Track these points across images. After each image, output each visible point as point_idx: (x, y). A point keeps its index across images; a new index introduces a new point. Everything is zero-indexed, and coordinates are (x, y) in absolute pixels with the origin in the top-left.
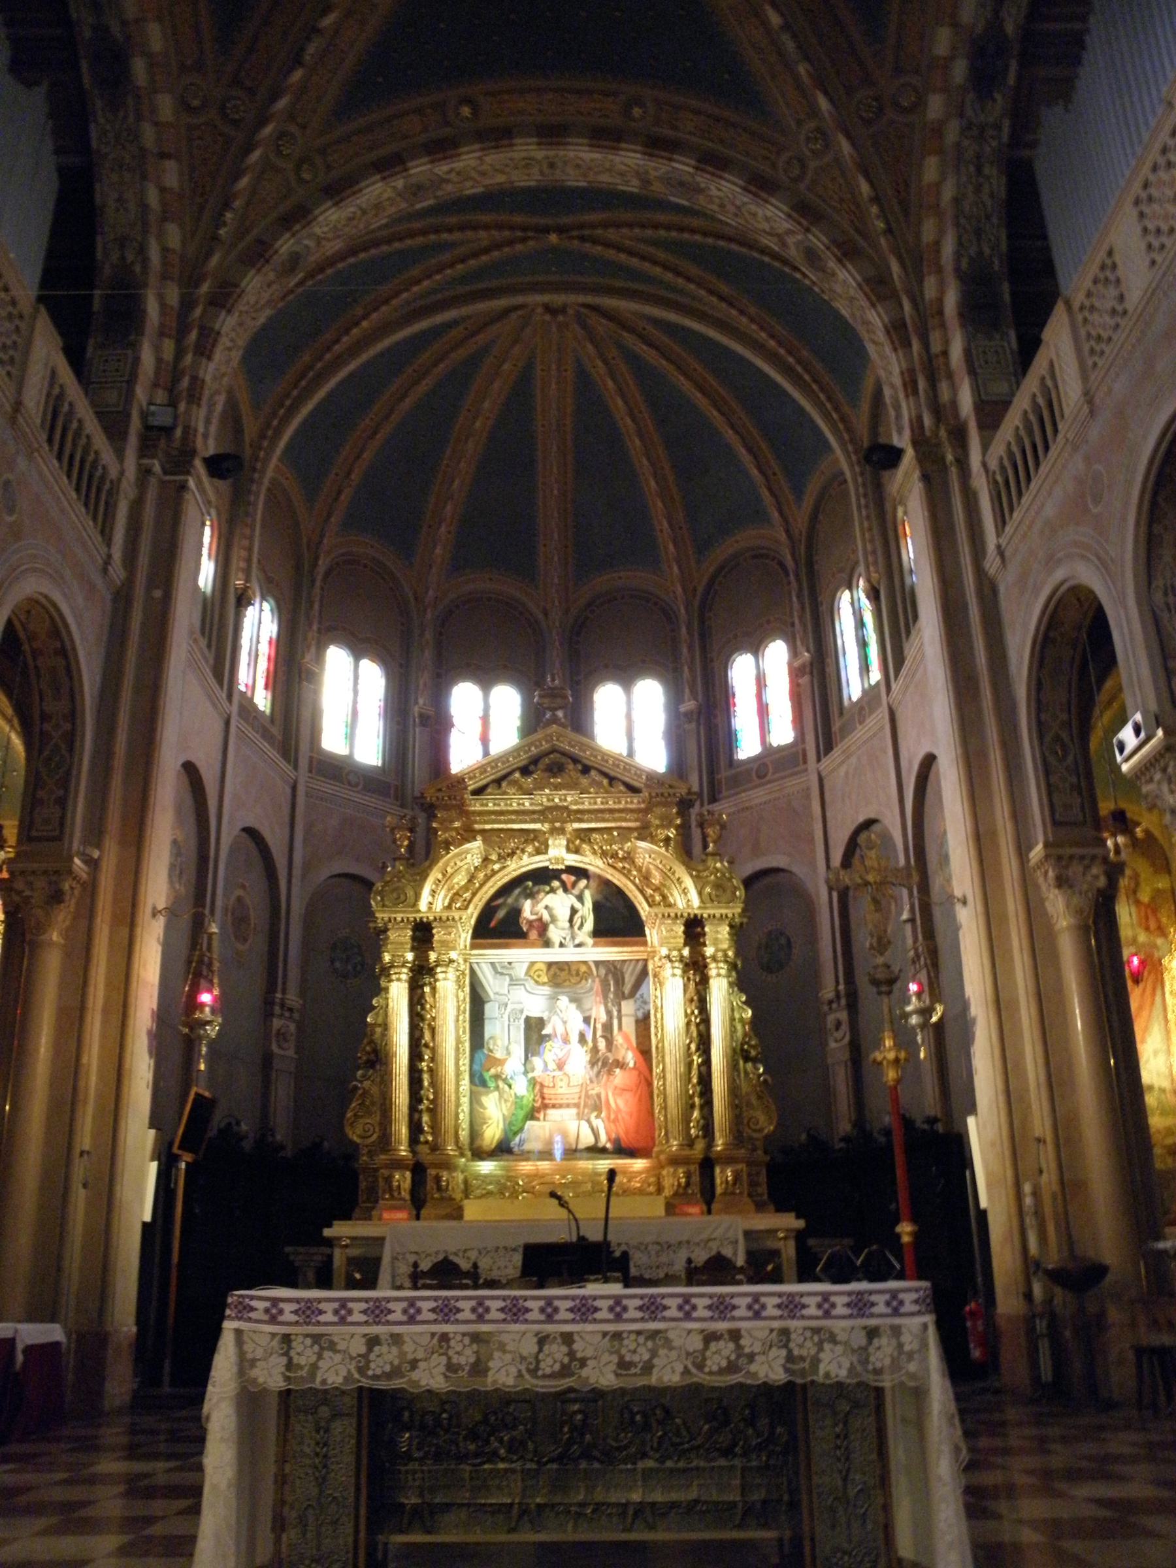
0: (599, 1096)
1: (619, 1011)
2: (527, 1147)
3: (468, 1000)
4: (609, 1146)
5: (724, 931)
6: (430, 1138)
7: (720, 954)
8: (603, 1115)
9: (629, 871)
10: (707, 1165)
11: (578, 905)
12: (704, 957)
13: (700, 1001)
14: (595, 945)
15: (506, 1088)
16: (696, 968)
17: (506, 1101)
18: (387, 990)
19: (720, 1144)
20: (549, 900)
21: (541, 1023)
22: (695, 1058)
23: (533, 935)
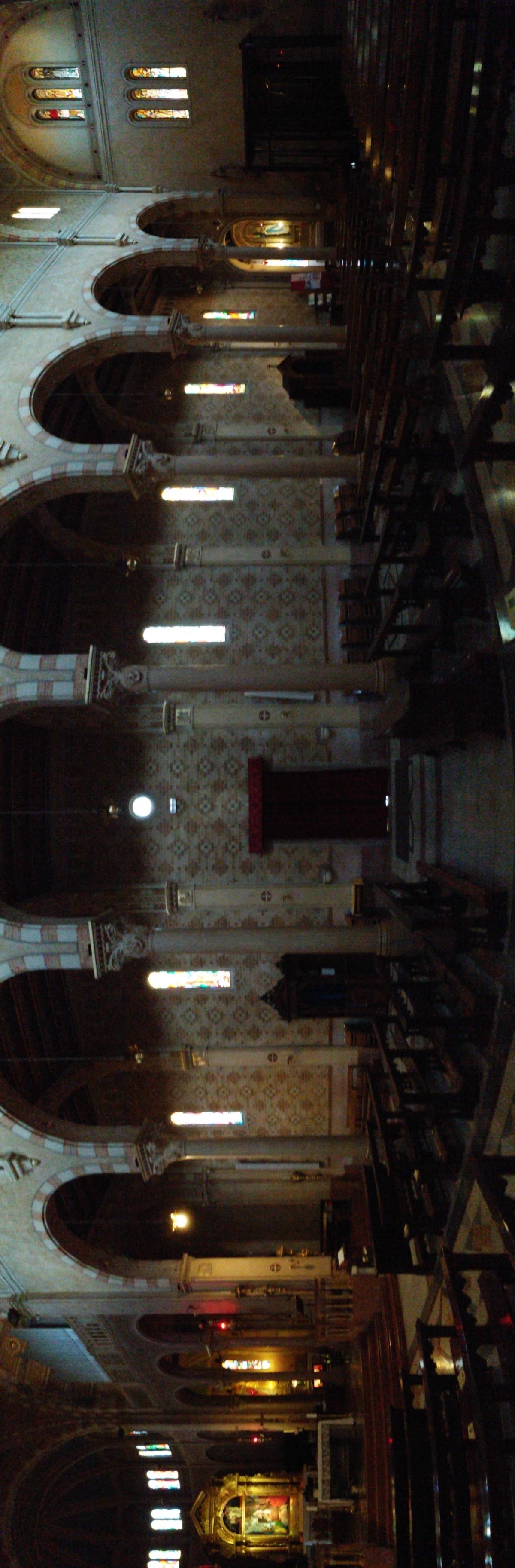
13: (256, 1484)
16: (249, 1484)
19: (288, 1481)
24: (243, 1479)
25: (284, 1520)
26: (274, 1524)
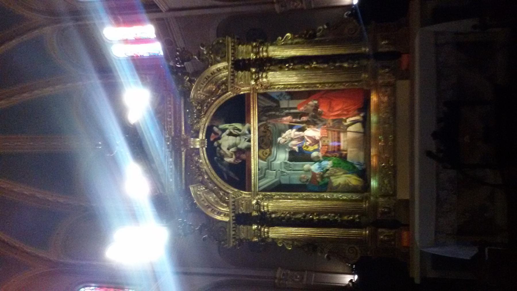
0: (333, 120)
1: (286, 109)
2: (362, 161)
3: (279, 193)
4: (362, 115)
5: (242, 48)
6: (357, 216)
7: (255, 50)
8: (344, 118)
9: (209, 103)
10: (378, 56)
11: (227, 132)
12: (256, 59)
14: (249, 122)
15: (328, 172)
17: (335, 173)
18: (273, 239)
20: (224, 148)
21: (292, 153)
22: (313, 66)
23: (244, 156)
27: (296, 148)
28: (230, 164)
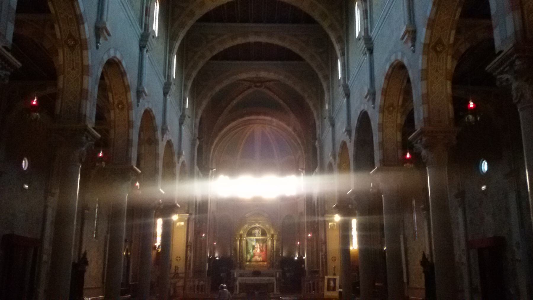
13: (273, 243)
14: (261, 236)
24: (275, 237)
25: (254, 259)
26: (252, 254)
27: (255, 247)
28: (252, 232)
